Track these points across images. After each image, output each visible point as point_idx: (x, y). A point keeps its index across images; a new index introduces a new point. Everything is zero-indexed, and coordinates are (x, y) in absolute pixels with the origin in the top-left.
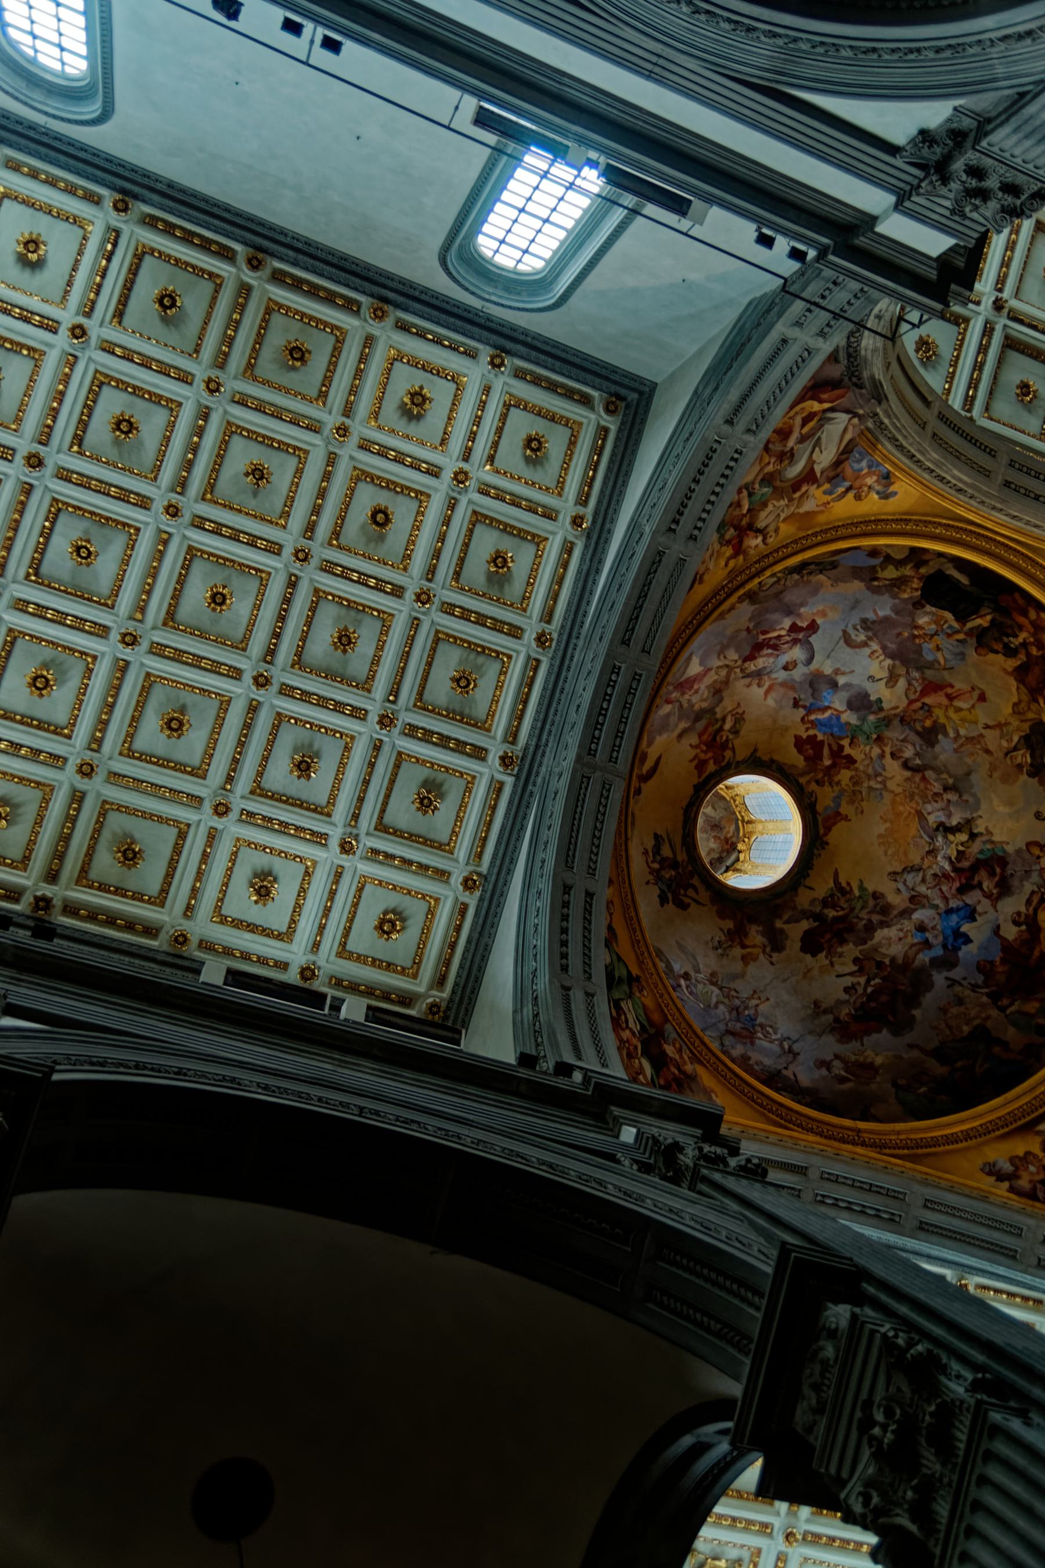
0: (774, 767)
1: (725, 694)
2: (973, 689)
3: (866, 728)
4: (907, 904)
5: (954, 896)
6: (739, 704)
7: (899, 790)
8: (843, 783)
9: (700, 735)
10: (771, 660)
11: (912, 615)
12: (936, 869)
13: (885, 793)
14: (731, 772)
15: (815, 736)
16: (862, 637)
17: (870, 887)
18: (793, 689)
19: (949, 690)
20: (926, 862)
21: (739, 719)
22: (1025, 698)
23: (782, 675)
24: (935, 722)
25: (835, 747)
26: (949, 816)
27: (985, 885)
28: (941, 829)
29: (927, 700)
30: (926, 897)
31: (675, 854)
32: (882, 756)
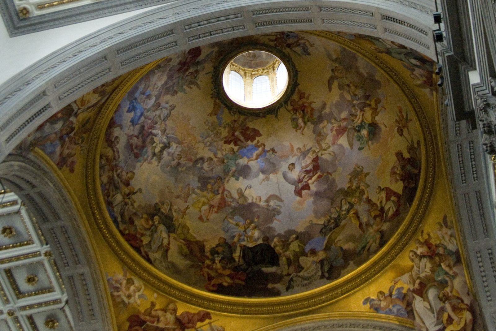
0: (261, 115)
1: (314, 136)
2: (208, 219)
3: (232, 162)
4: (160, 101)
5: (143, 122)
6: (302, 134)
7: (197, 146)
8: (222, 129)
9: (313, 110)
10: (304, 165)
11: (263, 232)
12: (158, 126)
13: (201, 139)
15: (252, 141)
16: (272, 203)
17: (180, 94)
18: (281, 157)
19: (215, 209)
20: (163, 125)
21: (296, 127)
22: (189, 236)
23: (292, 160)
24: (207, 190)
25: (239, 143)
26: (169, 154)
27: (135, 138)
28: (168, 145)
29: (219, 196)
30: (154, 111)
31: (291, 49)
32: (215, 155)
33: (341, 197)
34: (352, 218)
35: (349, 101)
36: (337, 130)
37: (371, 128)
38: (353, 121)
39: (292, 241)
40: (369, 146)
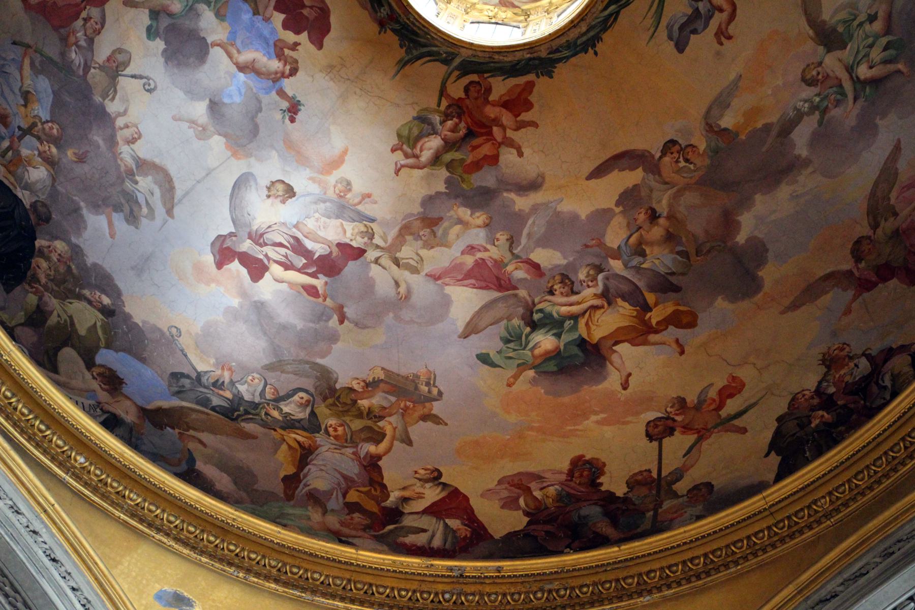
0: (384, 12)
1: (417, 209)
6: (397, 172)
9: (494, 160)
10: (311, 224)
14: (465, 53)
15: (286, 26)
23: (300, 180)
33: (308, 384)
34: (284, 447)
35: (601, 244)
36: (480, 264)
37: (575, 350)
38: (551, 292)
39: (90, 302)
40: (516, 377)
